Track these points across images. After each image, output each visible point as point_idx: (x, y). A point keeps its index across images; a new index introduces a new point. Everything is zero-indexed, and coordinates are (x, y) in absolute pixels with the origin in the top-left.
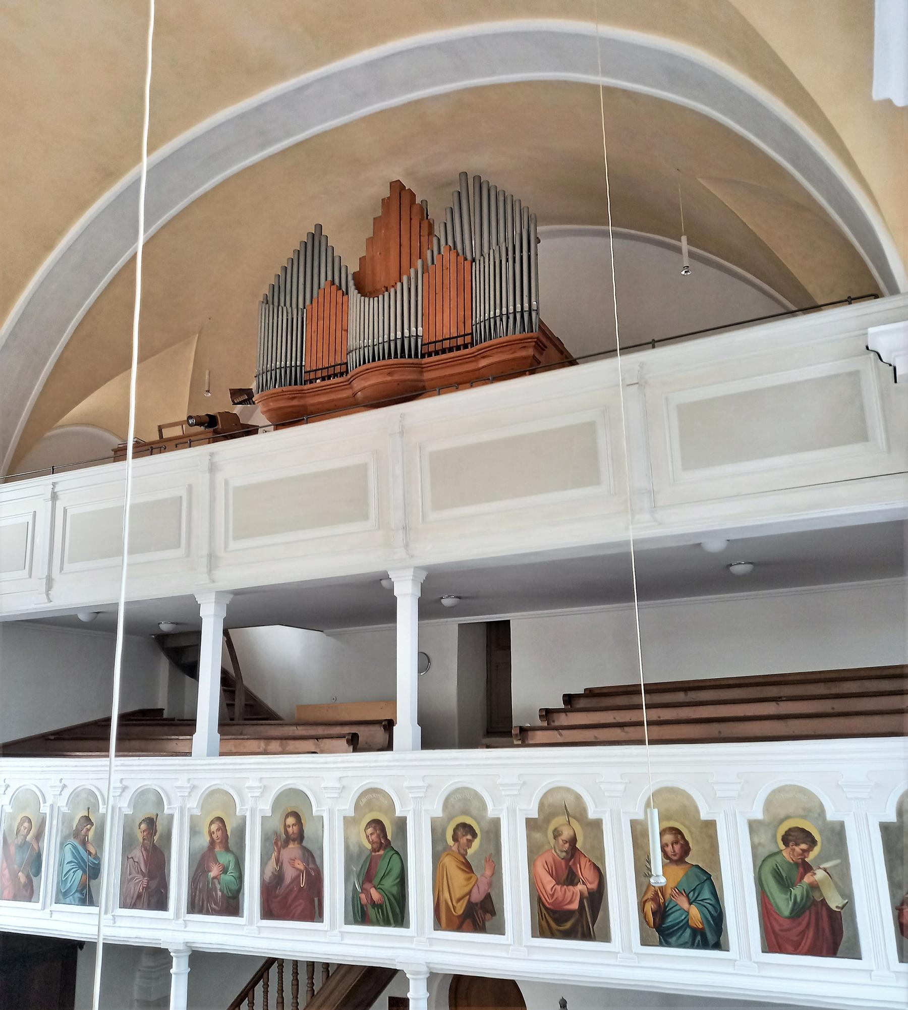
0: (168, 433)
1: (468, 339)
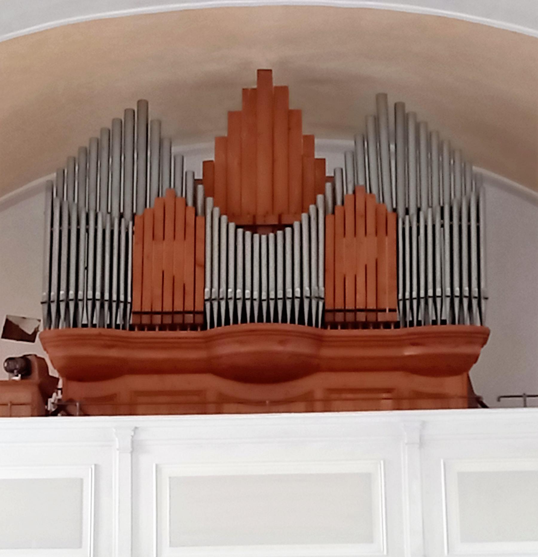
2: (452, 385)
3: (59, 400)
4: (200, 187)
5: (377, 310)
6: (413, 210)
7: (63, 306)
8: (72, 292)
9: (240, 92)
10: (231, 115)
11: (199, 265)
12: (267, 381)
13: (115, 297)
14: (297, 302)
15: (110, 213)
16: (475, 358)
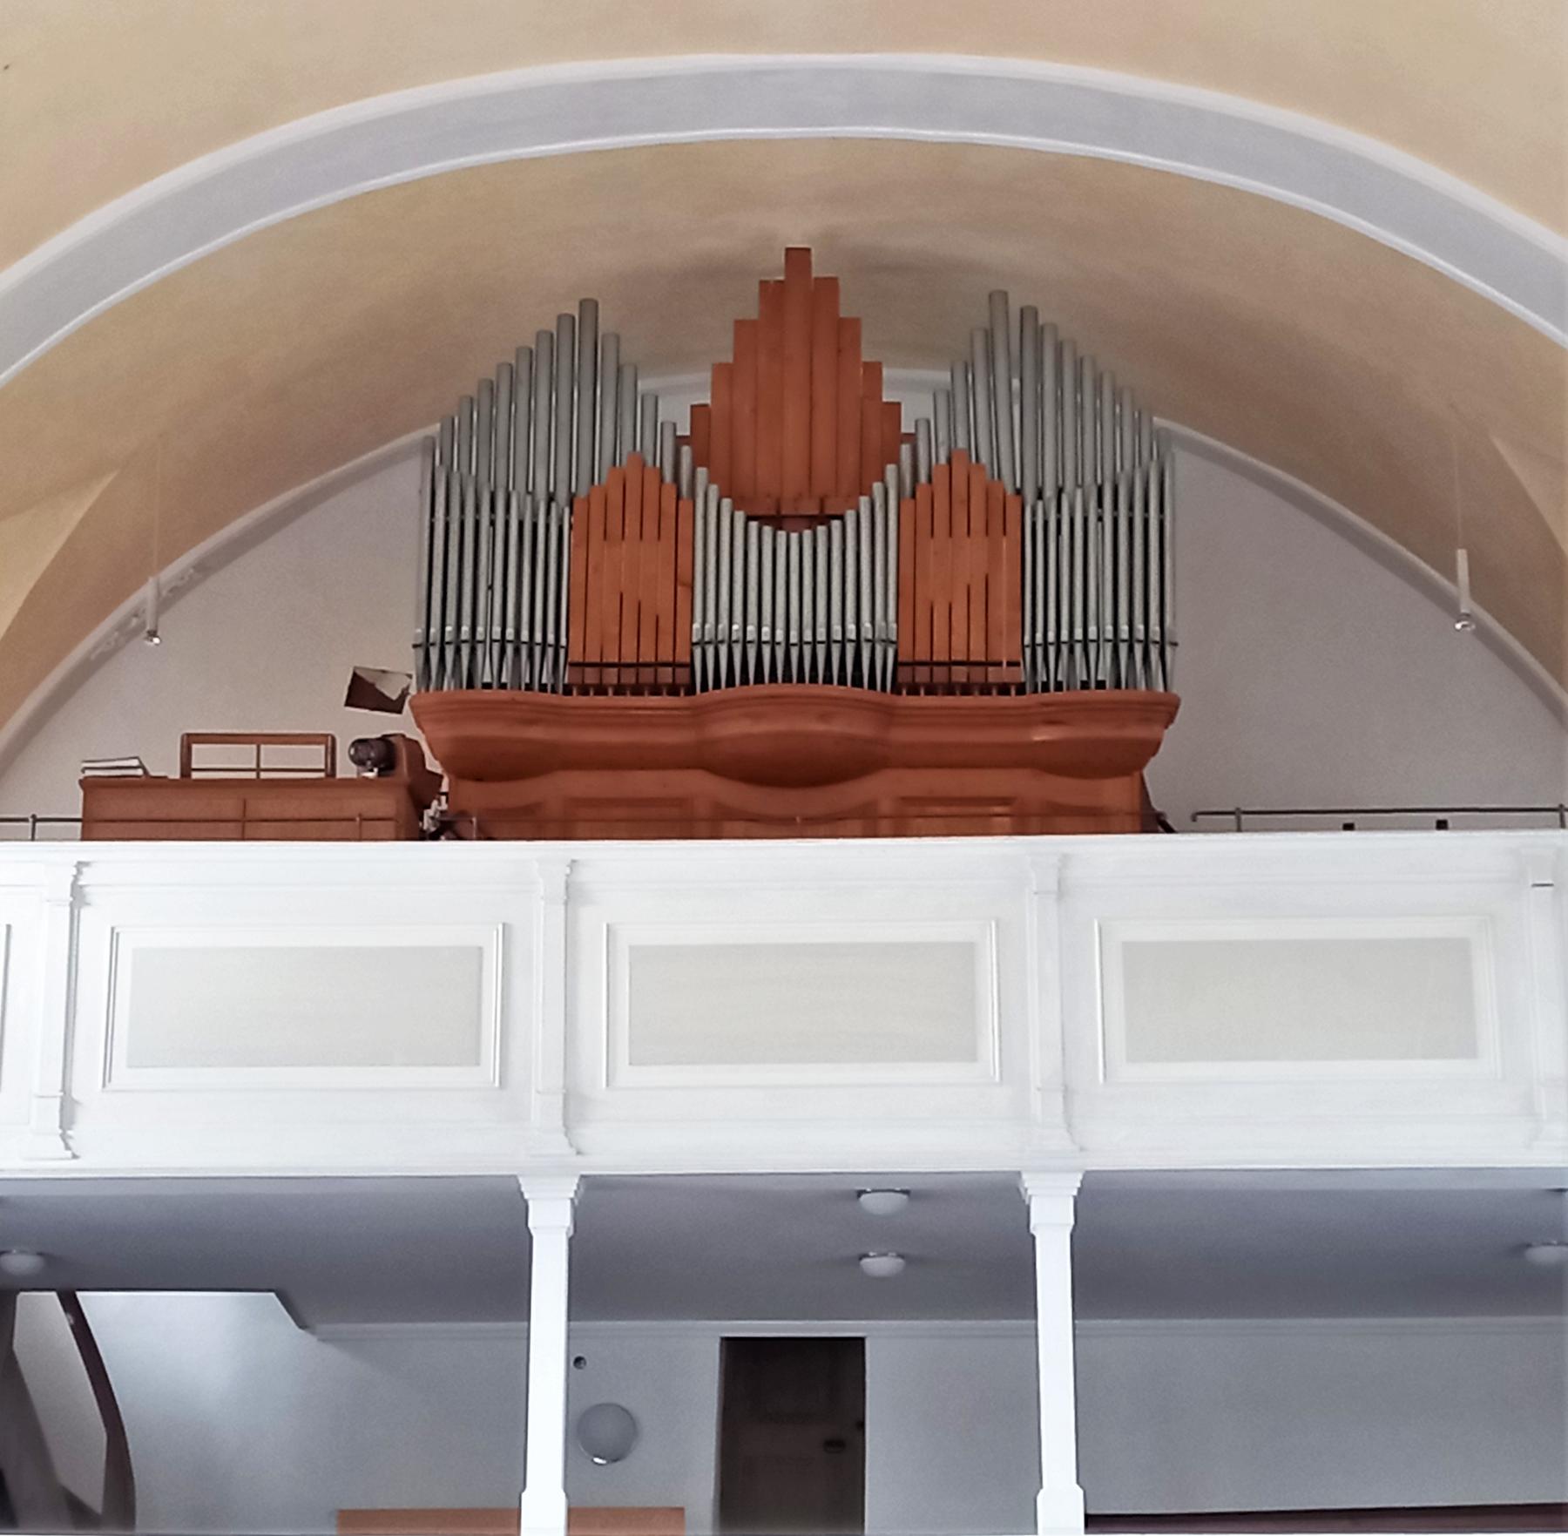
2: (1114, 792)
3: (442, 812)
4: (686, 450)
5: (986, 664)
6: (1049, 492)
7: (450, 652)
8: (465, 629)
9: (756, 289)
10: (740, 325)
11: (682, 582)
12: (797, 785)
13: (538, 637)
14: (850, 648)
15: (532, 494)
16: (1153, 747)
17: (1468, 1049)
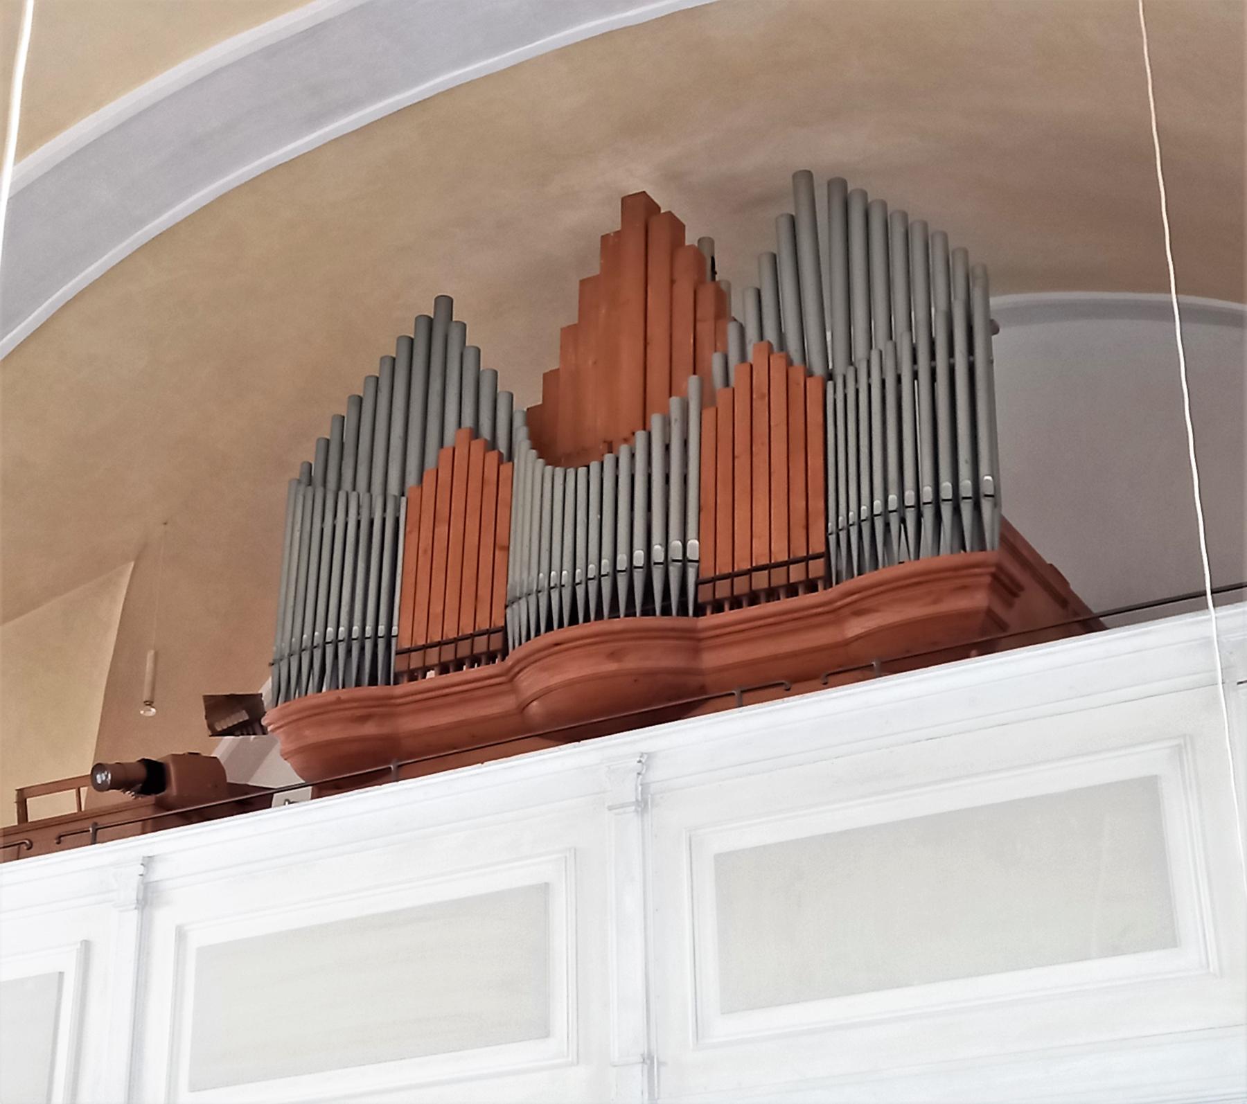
0: (40, 809)
1: (817, 568)
17: (1166, 936)
